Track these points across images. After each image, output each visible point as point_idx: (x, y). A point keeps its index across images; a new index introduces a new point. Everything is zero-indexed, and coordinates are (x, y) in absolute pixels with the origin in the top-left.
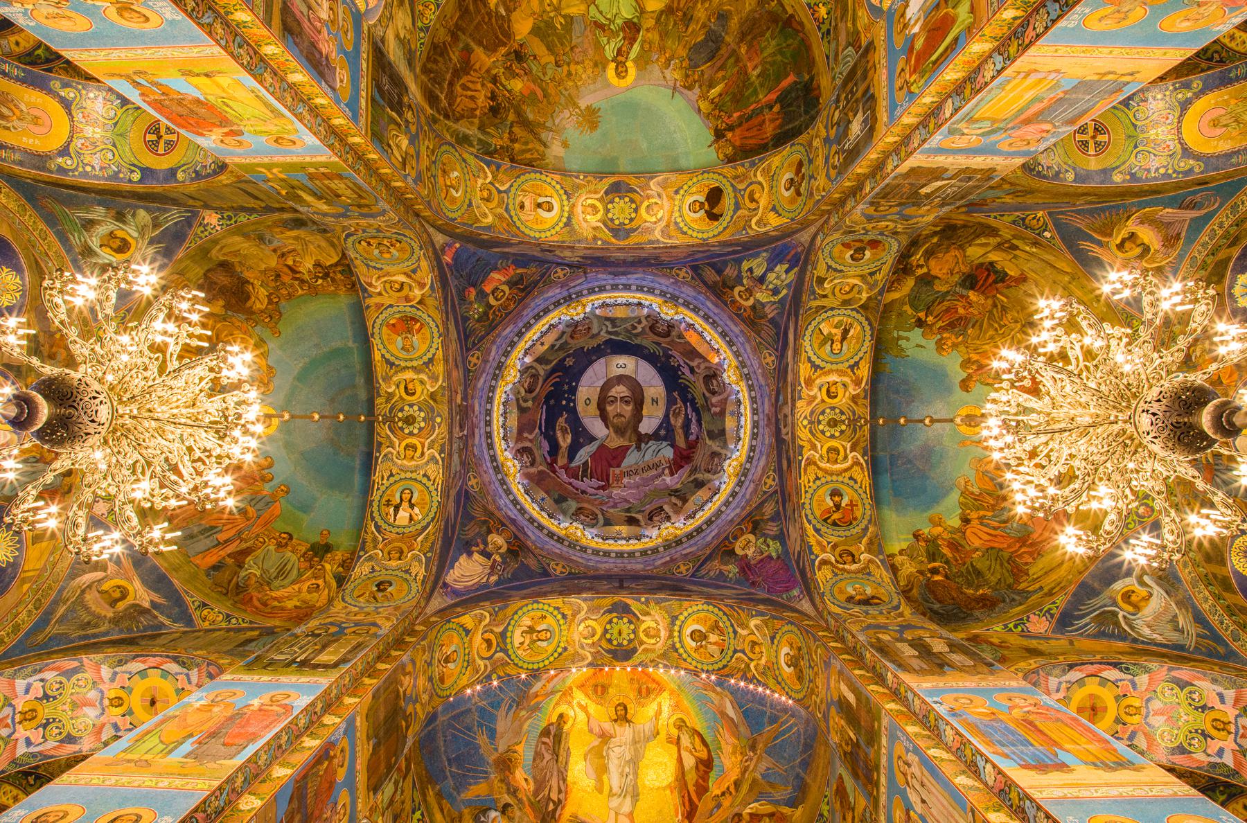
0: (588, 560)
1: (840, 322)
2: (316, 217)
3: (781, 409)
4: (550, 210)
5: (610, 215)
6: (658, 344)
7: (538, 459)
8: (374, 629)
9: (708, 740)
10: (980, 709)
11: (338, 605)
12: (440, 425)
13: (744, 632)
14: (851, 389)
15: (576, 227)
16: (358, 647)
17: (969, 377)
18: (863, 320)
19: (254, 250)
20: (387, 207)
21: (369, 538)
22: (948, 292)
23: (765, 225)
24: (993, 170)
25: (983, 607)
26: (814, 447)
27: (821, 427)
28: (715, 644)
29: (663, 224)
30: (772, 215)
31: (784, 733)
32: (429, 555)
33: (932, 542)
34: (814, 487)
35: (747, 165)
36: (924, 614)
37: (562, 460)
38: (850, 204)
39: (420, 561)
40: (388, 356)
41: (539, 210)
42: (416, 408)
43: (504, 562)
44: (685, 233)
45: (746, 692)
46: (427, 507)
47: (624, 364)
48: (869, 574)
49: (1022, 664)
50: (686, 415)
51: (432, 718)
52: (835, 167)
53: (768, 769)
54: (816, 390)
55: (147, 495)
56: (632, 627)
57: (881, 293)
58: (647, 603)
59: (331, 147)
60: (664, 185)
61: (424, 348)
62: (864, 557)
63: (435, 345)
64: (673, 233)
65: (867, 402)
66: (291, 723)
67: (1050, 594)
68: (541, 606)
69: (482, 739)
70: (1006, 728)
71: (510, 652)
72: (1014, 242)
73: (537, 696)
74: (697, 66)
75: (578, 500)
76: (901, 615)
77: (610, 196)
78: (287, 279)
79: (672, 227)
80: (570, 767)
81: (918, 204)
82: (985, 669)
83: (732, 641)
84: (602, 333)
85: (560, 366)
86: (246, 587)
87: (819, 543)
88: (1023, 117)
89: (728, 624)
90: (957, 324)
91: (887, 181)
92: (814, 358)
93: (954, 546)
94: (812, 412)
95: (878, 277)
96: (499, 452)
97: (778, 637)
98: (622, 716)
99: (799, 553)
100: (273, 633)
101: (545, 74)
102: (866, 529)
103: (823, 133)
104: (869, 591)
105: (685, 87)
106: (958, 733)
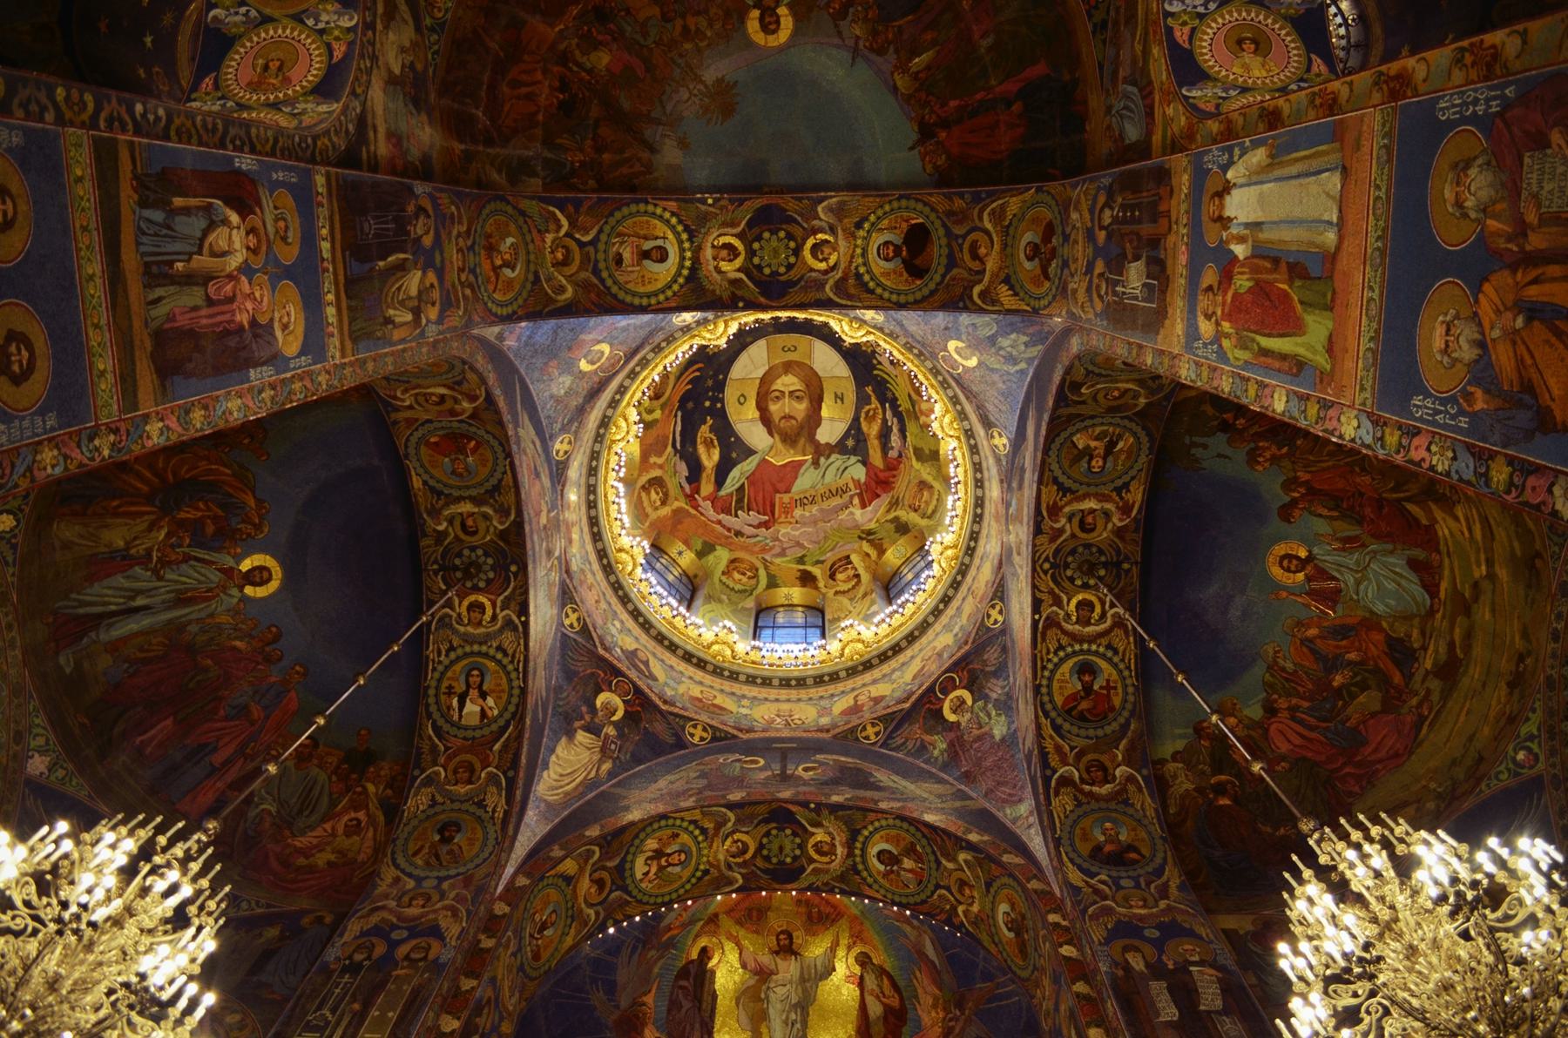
4: (662, 256)
5: (756, 260)
7: (673, 489)
9: (901, 983)
13: (950, 866)
14: (1115, 520)
17: (1294, 503)
18: (1138, 429)
21: (426, 748)
23: (994, 302)
26: (1058, 602)
27: (1069, 573)
28: (910, 871)
29: (838, 274)
30: (1004, 290)
34: (1056, 660)
37: (707, 487)
39: (498, 785)
40: (432, 483)
41: (647, 263)
42: (480, 552)
43: (621, 735)
44: (872, 292)
46: (505, 697)
48: (1126, 802)
50: (885, 420)
54: (1063, 521)
56: (798, 840)
57: (1167, 398)
60: (839, 211)
61: (487, 470)
64: (852, 291)
69: (598, 998)
73: (669, 929)
75: (728, 545)
76: (1164, 892)
77: (756, 230)
79: (851, 281)
83: (934, 873)
87: (1058, 749)
89: (929, 850)
92: (1062, 479)
94: (1057, 551)
98: (787, 948)
101: (645, 35)
102: (1125, 727)
105: (871, 49)
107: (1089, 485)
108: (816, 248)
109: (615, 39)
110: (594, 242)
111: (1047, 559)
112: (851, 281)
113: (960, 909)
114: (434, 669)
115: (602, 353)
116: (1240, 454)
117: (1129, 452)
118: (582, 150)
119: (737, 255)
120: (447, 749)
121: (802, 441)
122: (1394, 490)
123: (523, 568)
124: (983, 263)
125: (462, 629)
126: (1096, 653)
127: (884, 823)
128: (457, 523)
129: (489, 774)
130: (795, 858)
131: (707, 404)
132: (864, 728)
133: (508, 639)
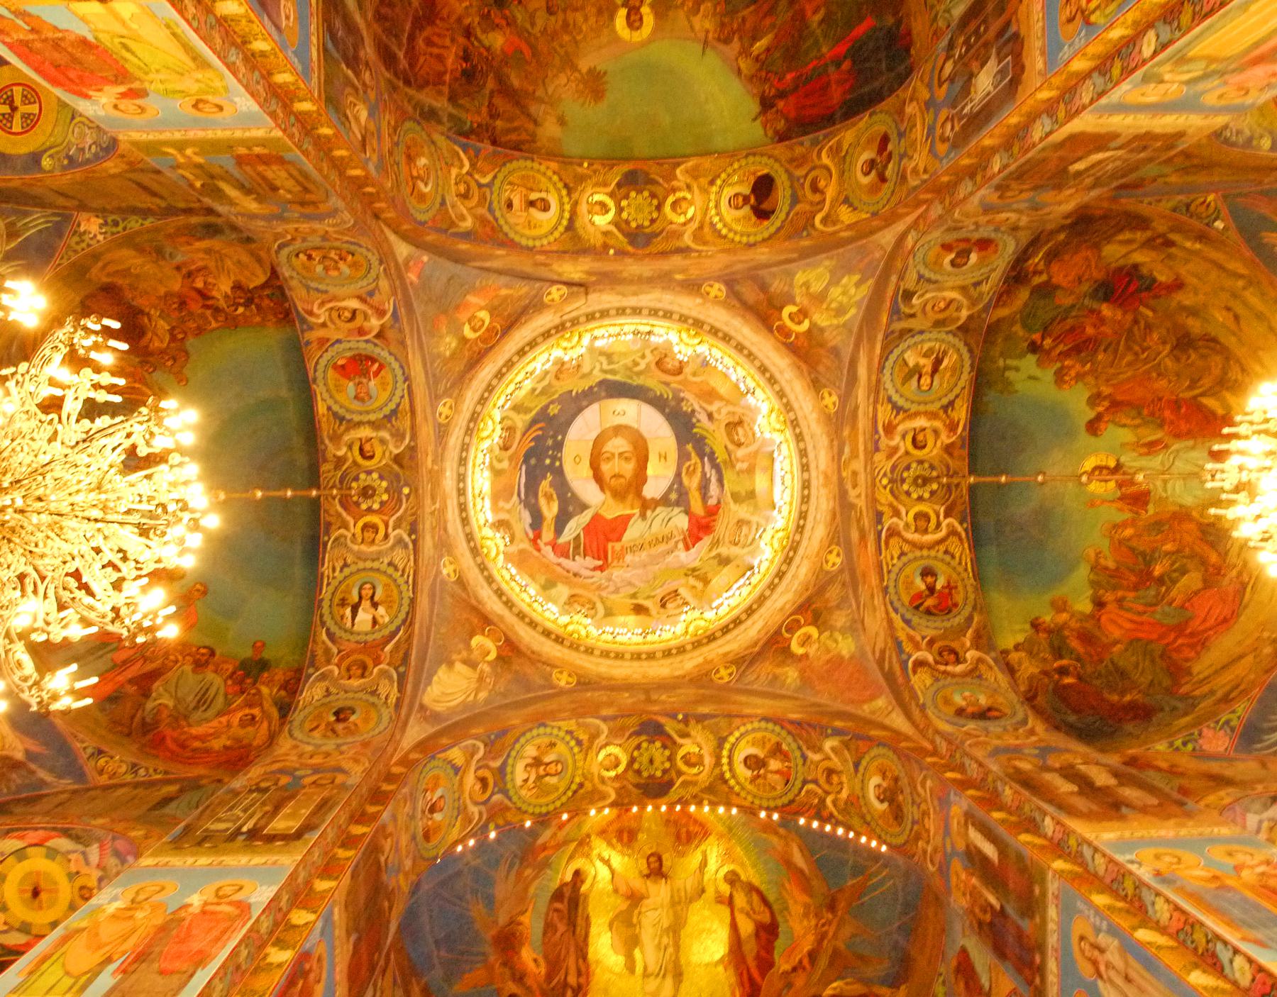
0: (598, 664)
1: (931, 350)
2: (240, 221)
3: (847, 463)
4: (546, 208)
5: (624, 215)
6: (667, 384)
7: (519, 534)
8: (340, 778)
9: (771, 897)
10: (1195, 870)
11: (284, 745)
12: (408, 496)
13: (816, 757)
15: (581, 232)
16: (324, 806)
17: (1099, 417)
18: (961, 345)
19: (149, 268)
20: (340, 204)
21: (320, 652)
22: (1073, 306)
23: (834, 224)
24: (1180, 135)
25: (1135, 718)
26: (897, 513)
27: (905, 487)
28: (777, 772)
29: (694, 225)
31: (875, 887)
32: (402, 669)
33: (1055, 633)
34: (900, 564)
35: (807, 144)
36: (1057, 728)
37: (548, 534)
38: (965, 187)
40: (335, 408)
41: (532, 210)
42: (375, 475)
45: (821, 834)
46: (396, 606)
47: (629, 411)
48: (980, 677)
49: (1211, 799)
50: (704, 474)
51: (416, 887)
52: (944, 139)
53: (854, 936)
54: (897, 440)
55: (40, 624)
56: (667, 753)
57: (986, 309)
58: (686, 721)
59: (273, 115)
60: (694, 174)
61: (384, 396)
62: (971, 655)
63: (399, 393)
65: (965, 452)
66: (250, 930)
67: (1227, 700)
68: (548, 730)
69: (477, 910)
70: (1245, 900)
71: (511, 793)
72: (1174, 237)
74: (734, 12)
76: (1032, 732)
77: (623, 191)
78: (196, 307)
80: (591, 940)
81: (1059, 187)
82: (1175, 809)
84: (596, 372)
85: (542, 417)
86: (156, 722)
87: (911, 639)
88: (1257, 52)
89: (794, 746)
90: (1082, 347)
91: (1029, 155)
92: (895, 398)
93: (1086, 638)
94: (894, 468)
95: (985, 288)
96: (476, 529)
97: (864, 763)
99: (883, 652)
100: (199, 787)
102: (970, 619)
103: (924, 94)
104: (983, 701)
105: (719, 39)
106: (1177, 908)
107: (919, 404)
108: (675, 205)
109: (508, 24)
110: (489, 185)
111: (885, 475)
112: (707, 229)
113: (829, 800)
114: (328, 584)
115: (483, 322)
116: (1048, 375)
117: (954, 369)
118: (479, 113)
119: (607, 211)
120: (339, 652)
121: (630, 497)
122: (1190, 388)
123: (415, 490)
124: (822, 193)
125: (356, 547)
126: (935, 558)
127: (749, 727)
128: (356, 449)
129: (381, 670)
130: (665, 771)
131: (548, 461)
132: (718, 671)
133: (399, 556)
